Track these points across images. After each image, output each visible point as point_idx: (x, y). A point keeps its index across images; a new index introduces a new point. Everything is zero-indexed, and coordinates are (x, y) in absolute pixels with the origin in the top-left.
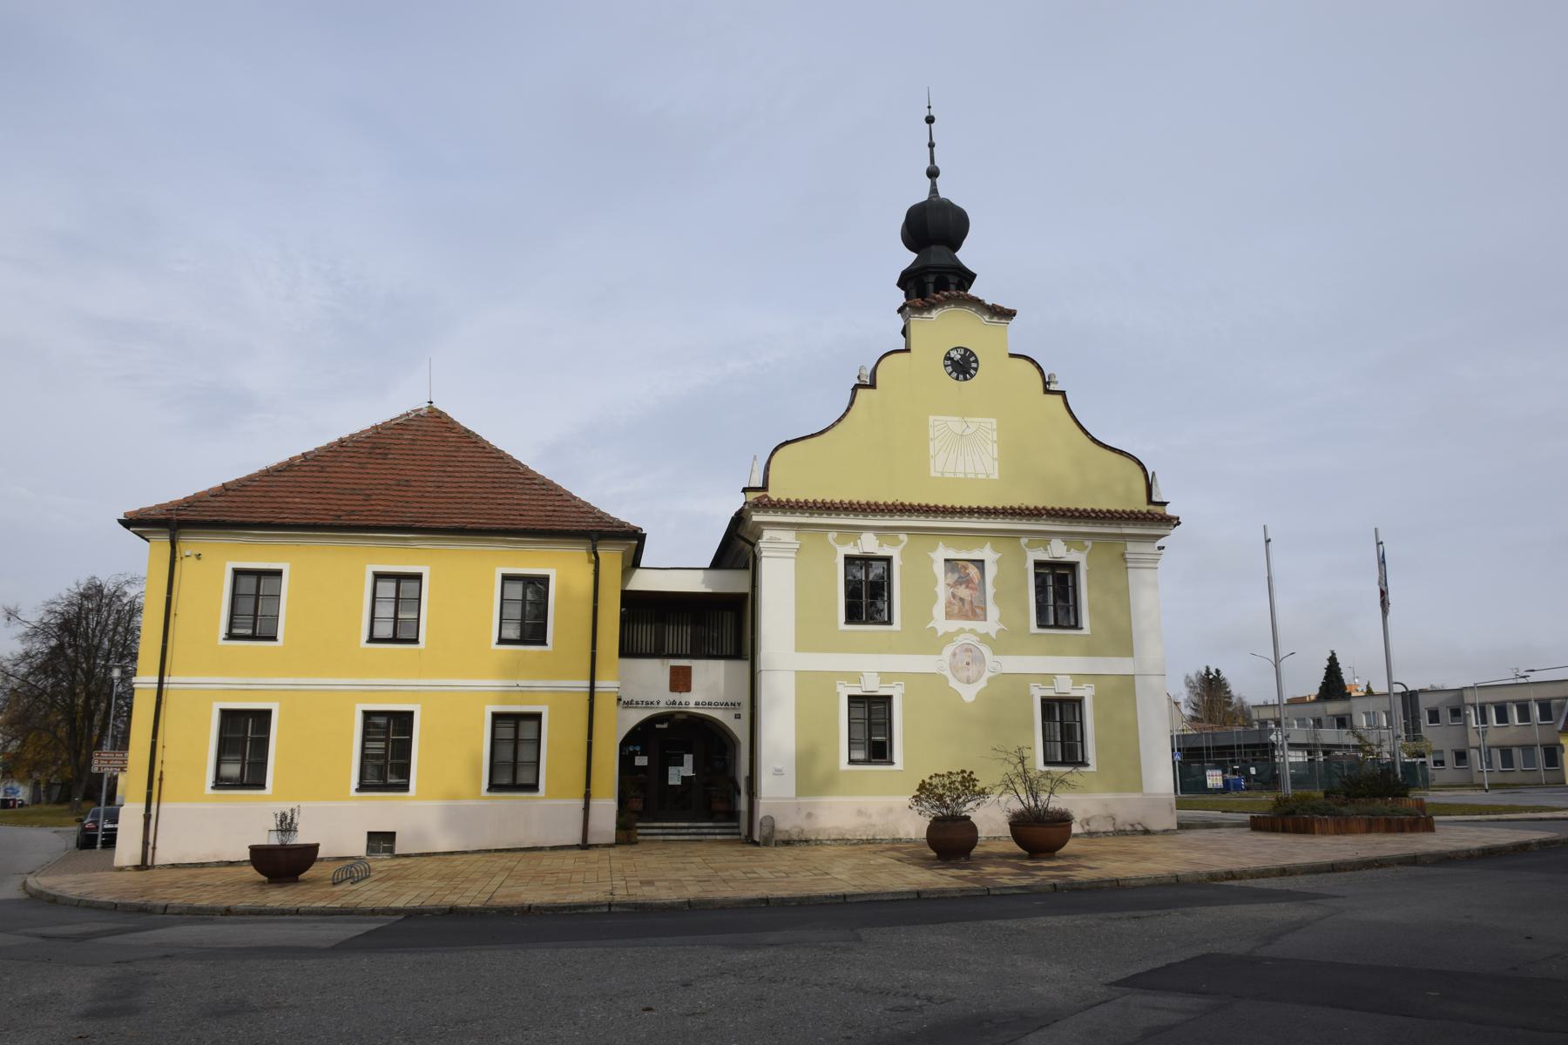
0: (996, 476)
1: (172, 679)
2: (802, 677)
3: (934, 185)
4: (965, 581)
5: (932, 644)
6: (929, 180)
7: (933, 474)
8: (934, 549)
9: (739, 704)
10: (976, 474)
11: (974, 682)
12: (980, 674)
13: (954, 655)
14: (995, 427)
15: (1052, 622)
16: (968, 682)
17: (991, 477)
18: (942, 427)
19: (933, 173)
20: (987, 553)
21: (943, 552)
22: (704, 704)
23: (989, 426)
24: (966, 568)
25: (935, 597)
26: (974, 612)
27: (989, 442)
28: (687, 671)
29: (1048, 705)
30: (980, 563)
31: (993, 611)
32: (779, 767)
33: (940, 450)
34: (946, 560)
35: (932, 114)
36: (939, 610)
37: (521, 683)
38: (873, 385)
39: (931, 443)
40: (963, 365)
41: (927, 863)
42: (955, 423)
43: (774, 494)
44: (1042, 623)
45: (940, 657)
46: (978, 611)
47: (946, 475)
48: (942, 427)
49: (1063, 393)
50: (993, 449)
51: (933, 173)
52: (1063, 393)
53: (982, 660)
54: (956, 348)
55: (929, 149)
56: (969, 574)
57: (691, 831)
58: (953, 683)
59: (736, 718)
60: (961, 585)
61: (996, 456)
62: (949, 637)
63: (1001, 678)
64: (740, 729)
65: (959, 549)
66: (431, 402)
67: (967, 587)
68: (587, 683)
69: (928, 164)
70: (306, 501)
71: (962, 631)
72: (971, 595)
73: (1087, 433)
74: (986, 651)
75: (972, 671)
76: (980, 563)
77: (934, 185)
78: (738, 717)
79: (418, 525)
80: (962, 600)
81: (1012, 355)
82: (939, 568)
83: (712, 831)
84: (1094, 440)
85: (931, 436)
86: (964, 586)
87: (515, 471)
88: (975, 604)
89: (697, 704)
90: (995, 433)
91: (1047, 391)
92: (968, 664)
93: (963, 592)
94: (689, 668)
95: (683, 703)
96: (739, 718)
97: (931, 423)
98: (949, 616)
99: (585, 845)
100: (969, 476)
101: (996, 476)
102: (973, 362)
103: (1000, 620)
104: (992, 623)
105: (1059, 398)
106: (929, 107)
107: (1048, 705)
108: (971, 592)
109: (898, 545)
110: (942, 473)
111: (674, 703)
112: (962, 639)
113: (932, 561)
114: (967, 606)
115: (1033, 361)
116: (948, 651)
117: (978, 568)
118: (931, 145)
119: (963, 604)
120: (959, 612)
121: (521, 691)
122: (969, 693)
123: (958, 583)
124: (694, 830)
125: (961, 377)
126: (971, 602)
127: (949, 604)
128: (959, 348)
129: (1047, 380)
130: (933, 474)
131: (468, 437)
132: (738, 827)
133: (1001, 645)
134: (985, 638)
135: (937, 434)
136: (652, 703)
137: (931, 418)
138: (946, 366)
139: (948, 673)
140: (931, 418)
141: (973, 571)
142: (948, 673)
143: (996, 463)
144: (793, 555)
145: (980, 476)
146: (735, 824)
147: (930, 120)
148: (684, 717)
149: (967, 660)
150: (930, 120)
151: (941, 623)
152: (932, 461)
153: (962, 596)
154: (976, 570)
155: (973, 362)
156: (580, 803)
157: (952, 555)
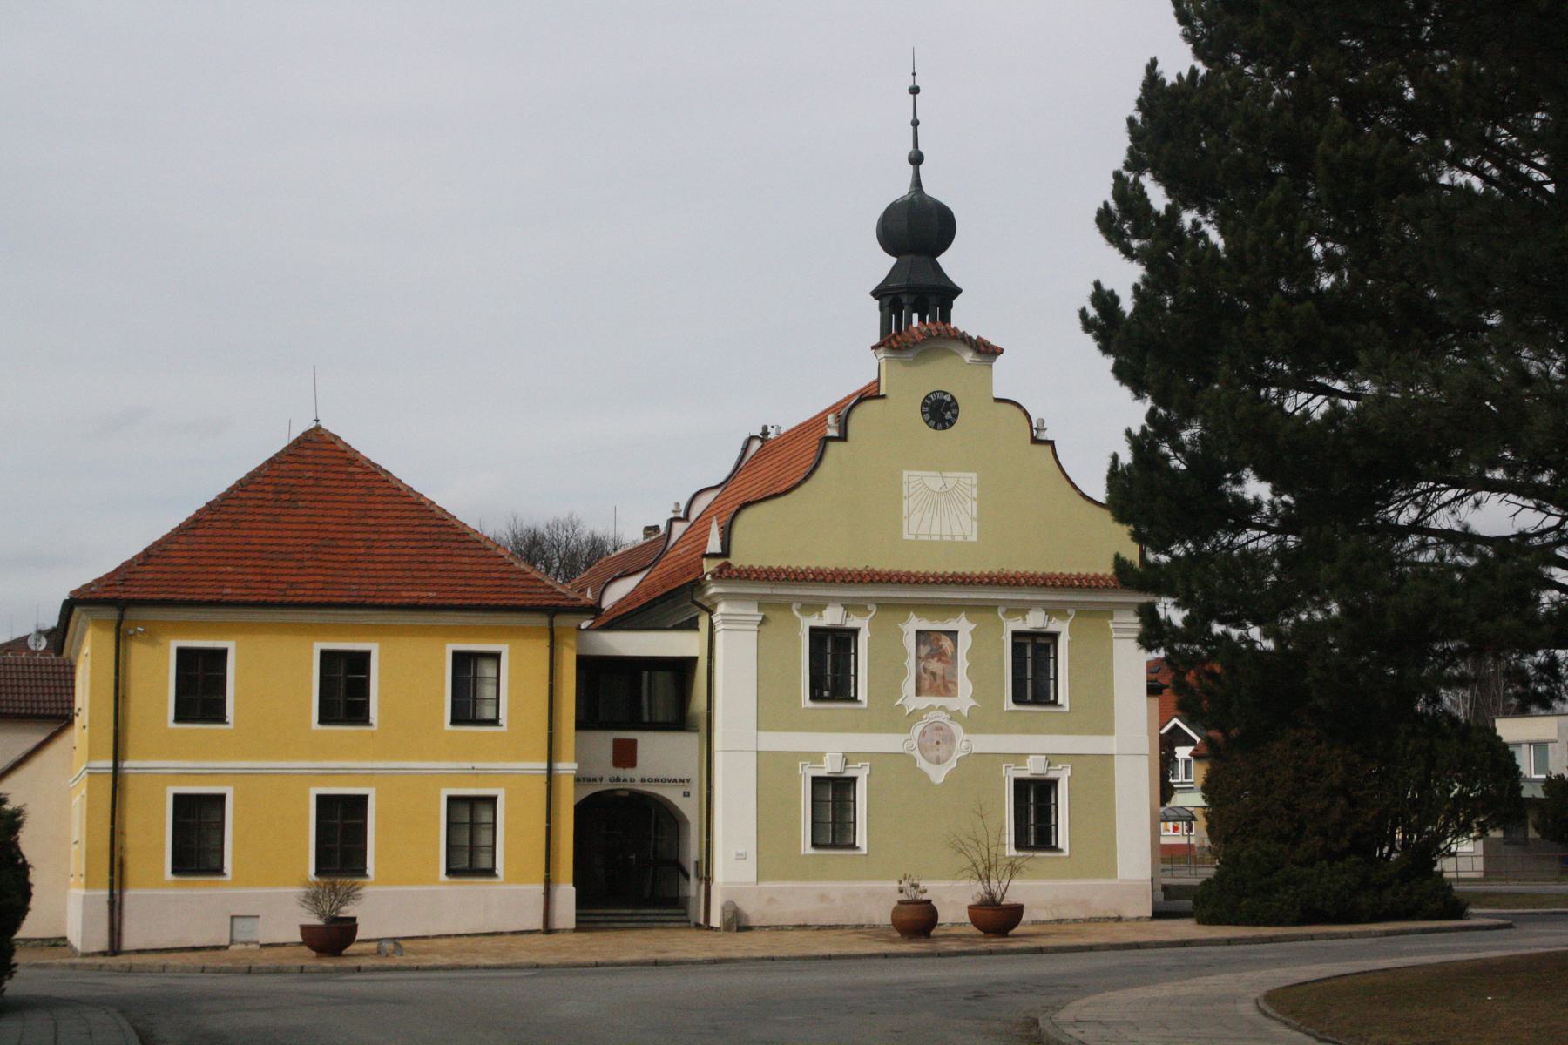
0: (974, 538)
1: (126, 764)
2: (765, 760)
3: (917, 175)
4: (938, 654)
5: (899, 721)
6: (911, 167)
7: (906, 536)
8: (905, 620)
9: (688, 781)
10: (953, 536)
11: (943, 762)
12: (950, 754)
13: (923, 733)
14: (975, 482)
15: (1029, 697)
16: (938, 761)
17: (969, 539)
18: (918, 484)
19: (916, 159)
20: (963, 625)
21: (915, 623)
22: (650, 780)
23: (968, 481)
24: (938, 640)
25: (905, 654)
26: (945, 687)
27: (969, 500)
28: (633, 744)
29: (1021, 786)
30: (953, 635)
31: (964, 686)
32: (741, 851)
33: (914, 510)
34: (918, 632)
35: (916, 84)
36: (909, 685)
37: (478, 765)
38: (843, 437)
39: (905, 502)
40: (940, 412)
41: (892, 941)
42: (933, 480)
43: (738, 559)
44: (1018, 698)
45: (908, 736)
46: (950, 686)
47: (921, 538)
48: (918, 484)
49: (1051, 443)
50: (972, 507)
51: (916, 159)
52: (1051, 443)
53: (950, 739)
54: (935, 392)
55: (912, 128)
56: (941, 647)
57: (635, 918)
58: (923, 764)
59: (684, 795)
60: (933, 657)
61: (975, 515)
62: (916, 715)
63: (974, 760)
64: (689, 808)
65: (931, 620)
66: (317, 421)
67: (940, 660)
68: (544, 765)
69: (910, 147)
70: (241, 570)
71: (931, 708)
72: (944, 670)
73: (1076, 488)
74: (957, 729)
75: (942, 751)
76: (953, 635)
77: (917, 175)
78: (686, 794)
79: (369, 601)
80: (933, 674)
81: (998, 400)
82: (910, 642)
83: (657, 918)
84: (1083, 495)
85: (905, 493)
86: (936, 659)
87: (442, 523)
88: (947, 678)
89: (643, 780)
90: (975, 490)
91: (1035, 441)
92: (938, 743)
93: (935, 665)
94: (634, 743)
95: (628, 780)
96: (689, 795)
97: (905, 479)
98: (918, 692)
99: (548, 930)
100: (945, 538)
101: (974, 538)
103: (973, 696)
104: (964, 697)
105: (1049, 448)
106: (914, 74)
107: (1021, 786)
108: (943, 665)
109: (867, 615)
110: (916, 535)
111: (618, 779)
113: (901, 634)
114: (939, 681)
115: (1019, 406)
116: (918, 729)
117: (951, 639)
118: (915, 123)
119: (935, 679)
120: (930, 688)
121: (476, 774)
122: (938, 775)
123: (931, 656)
124: (639, 918)
125: (940, 426)
126: (944, 677)
127: (918, 679)
128: (938, 392)
129: (1035, 426)
130: (906, 536)
131: (332, 443)
132: (685, 914)
133: (974, 723)
134: (955, 716)
135: (911, 493)
136: (595, 780)
137: (906, 473)
138: (923, 413)
139: (916, 753)
140: (906, 473)
141: (946, 643)
142: (916, 753)
143: (975, 524)
144: (756, 627)
145: (957, 539)
146: (682, 911)
147: (915, 91)
148: (627, 794)
149: (936, 739)
150: (915, 91)
151: (911, 701)
154: (950, 642)
156: (541, 887)
157: (925, 625)
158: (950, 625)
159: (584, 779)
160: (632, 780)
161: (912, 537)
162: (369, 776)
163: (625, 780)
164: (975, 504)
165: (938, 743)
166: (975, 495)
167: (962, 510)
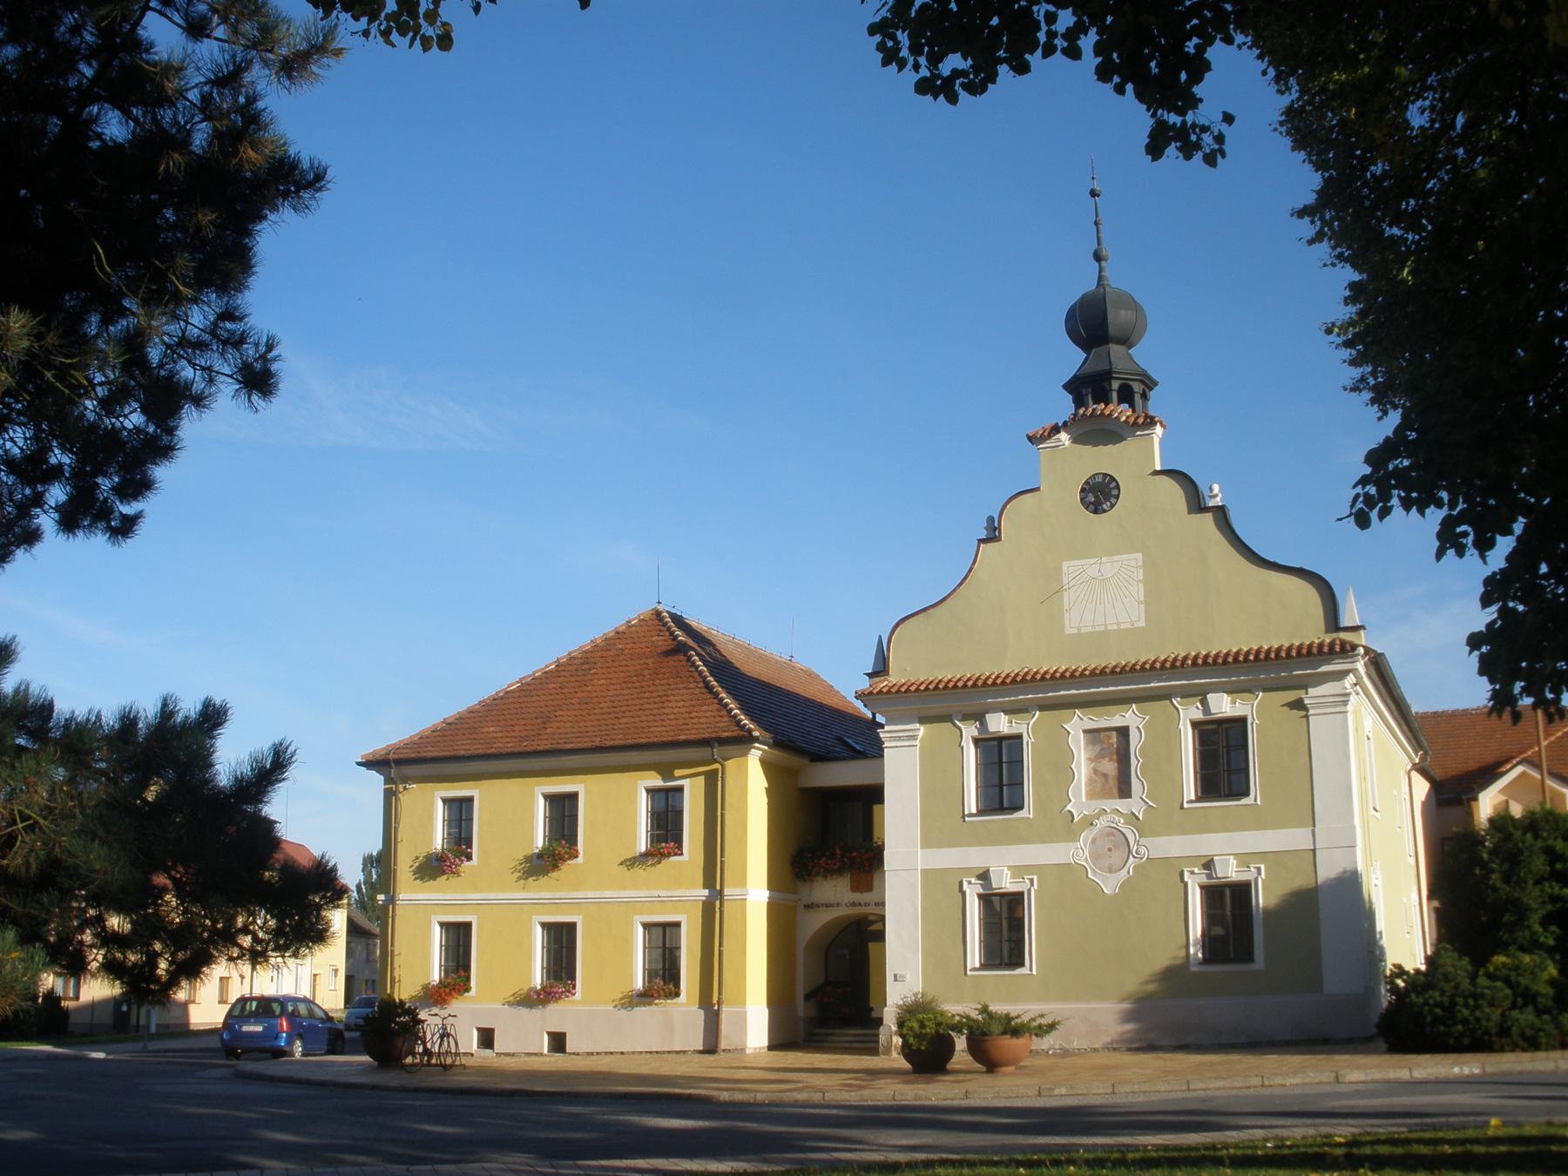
0: (1142, 623)
5: (1069, 829)
13: (1094, 840)
14: (1140, 564)
16: (1110, 871)
50: (1138, 591)
60: (1103, 758)
61: (1142, 599)
75: (1117, 857)
86: (1107, 759)
98: (1092, 795)
101: (1142, 623)
102: (1114, 488)
111: (854, 904)
112: (1101, 823)
116: (1086, 837)
119: (1107, 780)
121: (662, 901)
122: (1109, 885)
127: (1091, 782)
143: (1142, 607)
152: (1067, 615)
153: (1105, 771)
155: (1114, 488)
158: (1117, 721)
159: (822, 904)
160: (867, 904)
161: (1075, 631)
162: (577, 905)
163: (860, 905)
164: (1141, 585)
165: (1110, 850)
166: (1141, 578)
167: (1126, 593)
